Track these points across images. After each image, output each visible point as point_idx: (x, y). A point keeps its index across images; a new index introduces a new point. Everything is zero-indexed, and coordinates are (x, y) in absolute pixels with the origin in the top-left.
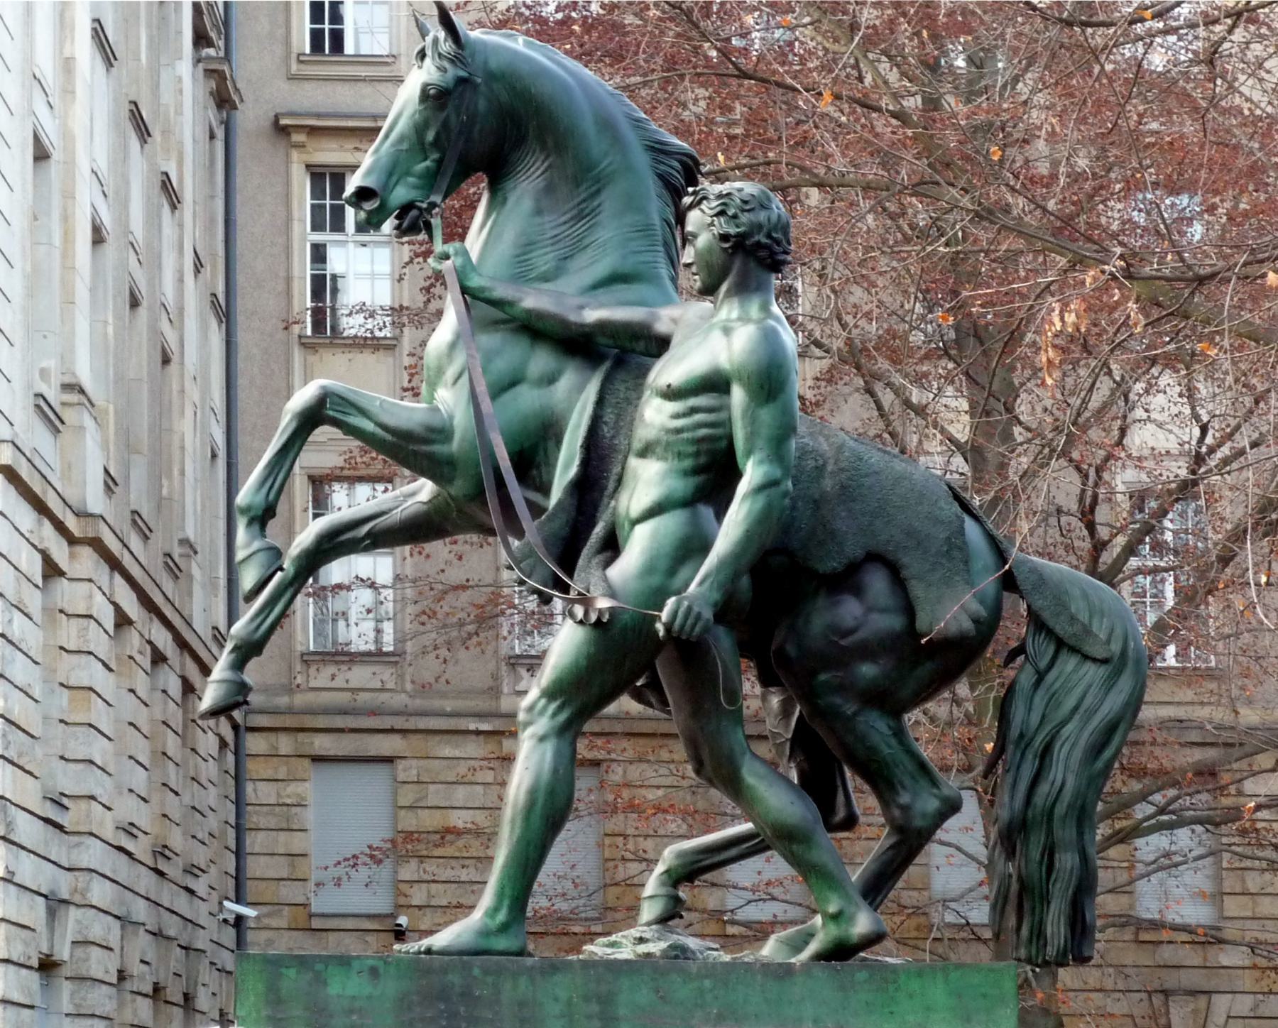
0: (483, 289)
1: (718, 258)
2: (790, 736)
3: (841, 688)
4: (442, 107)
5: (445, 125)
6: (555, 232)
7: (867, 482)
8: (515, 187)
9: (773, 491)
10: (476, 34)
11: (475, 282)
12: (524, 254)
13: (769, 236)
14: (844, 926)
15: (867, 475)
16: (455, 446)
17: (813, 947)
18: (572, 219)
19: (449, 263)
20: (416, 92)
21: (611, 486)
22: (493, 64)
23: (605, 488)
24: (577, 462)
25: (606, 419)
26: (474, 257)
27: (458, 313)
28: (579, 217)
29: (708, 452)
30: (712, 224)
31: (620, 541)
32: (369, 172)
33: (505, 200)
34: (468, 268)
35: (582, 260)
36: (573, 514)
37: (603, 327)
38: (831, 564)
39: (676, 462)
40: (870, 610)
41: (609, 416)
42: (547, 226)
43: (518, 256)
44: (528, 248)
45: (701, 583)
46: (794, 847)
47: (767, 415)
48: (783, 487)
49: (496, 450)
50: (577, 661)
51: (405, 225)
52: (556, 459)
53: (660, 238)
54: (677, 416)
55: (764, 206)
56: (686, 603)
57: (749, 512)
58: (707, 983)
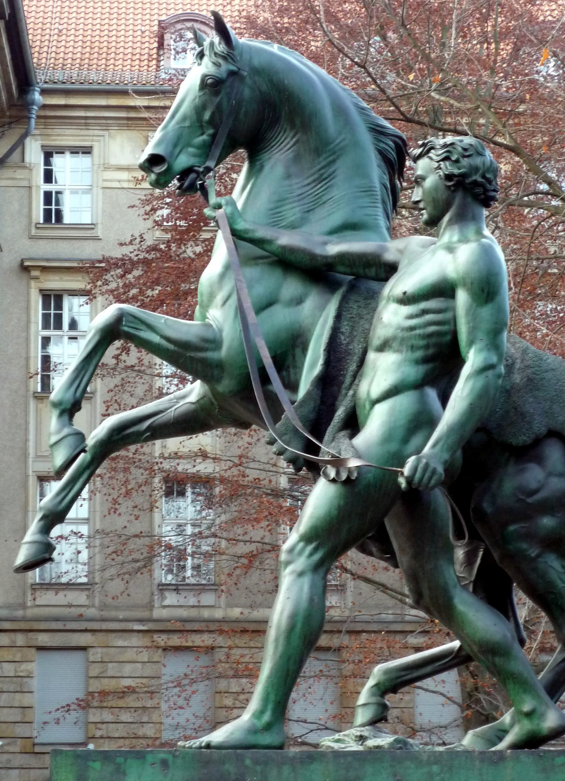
0: (246, 231)
1: (443, 195)
2: (473, 578)
3: (528, 536)
4: (216, 93)
5: (218, 109)
6: (300, 192)
7: (548, 375)
8: (270, 158)
9: (490, 373)
10: (243, 40)
11: (241, 225)
12: (277, 208)
13: (484, 177)
14: (536, 721)
15: (547, 371)
16: (224, 353)
17: (509, 739)
18: (314, 181)
19: (221, 211)
20: (197, 82)
21: (348, 380)
22: (256, 62)
23: (343, 383)
24: (321, 361)
25: (343, 330)
26: (240, 205)
27: (228, 248)
28: (320, 180)
29: (436, 345)
30: (439, 168)
31: (361, 419)
32: (159, 143)
33: (262, 167)
34: (236, 214)
35: (321, 212)
36: (318, 402)
37: (342, 257)
38: (523, 439)
39: (409, 353)
40: (550, 474)
41: (345, 328)
42: (296, 187)
43: (271, 210)
44: (280, 203)
45: (434, 446)
46: (497, 660)
47: (486, 312)
48: (497, 371)
49: (261, 351)
50: (330, 511)
51: (186, 184)
52: (303, 364)
53: (379, 197)
54: (411, 317)
55: (480, 154)
56: (424, 461)
57: (472, 390)
58: (435, 768)
